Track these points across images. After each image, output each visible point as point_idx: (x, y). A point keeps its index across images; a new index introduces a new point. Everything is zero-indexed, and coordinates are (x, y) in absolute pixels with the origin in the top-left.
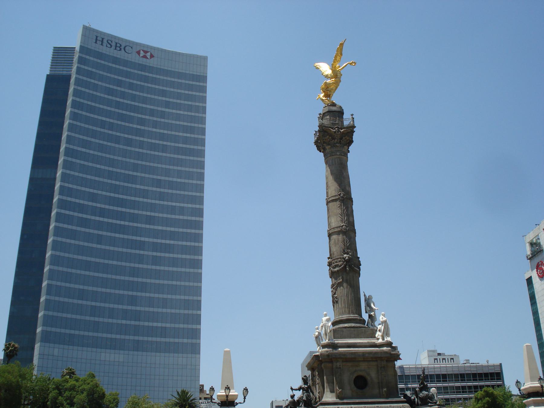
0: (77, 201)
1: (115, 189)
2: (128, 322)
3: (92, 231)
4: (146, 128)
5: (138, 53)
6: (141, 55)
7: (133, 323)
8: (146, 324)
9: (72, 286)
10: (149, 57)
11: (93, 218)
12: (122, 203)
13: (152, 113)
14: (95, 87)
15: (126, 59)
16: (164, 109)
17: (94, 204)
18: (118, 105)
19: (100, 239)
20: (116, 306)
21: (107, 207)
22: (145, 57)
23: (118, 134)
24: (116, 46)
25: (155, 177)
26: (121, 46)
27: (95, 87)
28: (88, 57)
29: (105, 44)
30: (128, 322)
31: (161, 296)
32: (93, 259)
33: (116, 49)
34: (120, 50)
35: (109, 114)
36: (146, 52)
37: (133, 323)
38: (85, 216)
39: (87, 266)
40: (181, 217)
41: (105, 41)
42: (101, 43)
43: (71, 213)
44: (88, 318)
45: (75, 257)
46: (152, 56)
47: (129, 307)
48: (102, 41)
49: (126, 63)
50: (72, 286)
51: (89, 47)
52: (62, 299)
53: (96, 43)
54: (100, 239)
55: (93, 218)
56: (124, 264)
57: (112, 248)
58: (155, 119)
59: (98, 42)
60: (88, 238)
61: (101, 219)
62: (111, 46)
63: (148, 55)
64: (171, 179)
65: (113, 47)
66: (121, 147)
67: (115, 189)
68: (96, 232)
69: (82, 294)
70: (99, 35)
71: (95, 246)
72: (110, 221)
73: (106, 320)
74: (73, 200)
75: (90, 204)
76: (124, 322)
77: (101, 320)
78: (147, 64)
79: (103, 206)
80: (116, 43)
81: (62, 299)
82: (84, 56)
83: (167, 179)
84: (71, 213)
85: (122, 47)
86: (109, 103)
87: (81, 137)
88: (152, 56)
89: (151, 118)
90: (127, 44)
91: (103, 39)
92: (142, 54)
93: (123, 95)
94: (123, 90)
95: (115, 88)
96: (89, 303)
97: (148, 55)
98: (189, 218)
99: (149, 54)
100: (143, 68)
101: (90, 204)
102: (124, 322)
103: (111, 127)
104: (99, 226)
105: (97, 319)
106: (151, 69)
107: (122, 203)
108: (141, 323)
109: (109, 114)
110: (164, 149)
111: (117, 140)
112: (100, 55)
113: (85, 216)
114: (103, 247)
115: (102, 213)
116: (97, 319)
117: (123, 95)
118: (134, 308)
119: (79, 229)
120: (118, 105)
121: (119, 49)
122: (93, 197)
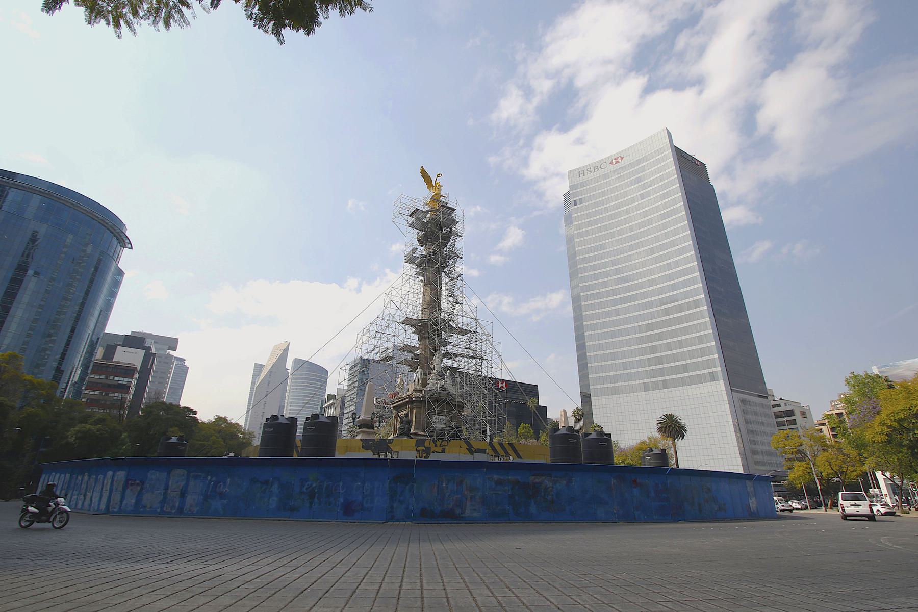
1: (619, 271)
5: (612, 163)
9: (605, 352)
19: (617, 312)
22: (617, 162)
31: (676, 339)
32: (616, 329)
39: (613, 334)
40: (677, 269)
44: (622, 372)
45: (603, 331)
47: (652, 356)
50: (605, 352)
52: (600, 364)
54: (617, 312)
57: (628, 315)
60: (608, 314)
69: (614, 356)
71: (615, 318)
72: (622, 296)
73: (636, 370)
77: (632, 371)
81: (600, 364)
92: (614, 161)
96: (620, 361)
98: (684, 267)
104: (615, 303)
105: (629, 371)
118: (656, 355)
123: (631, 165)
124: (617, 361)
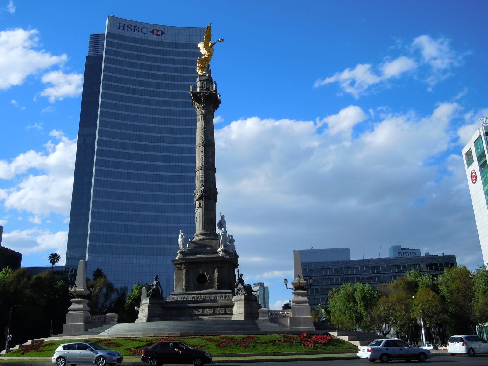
0: (111, 149)
1: (140, 138)
2: (152, 235)
3: (123, 170)
4: (161, 90)
5: (152, 32)
6: (155, 34)
7: (156, 235)
8: (166, 235)
9: (110, 211)
10: (160, 34)
11: (124, 161)
12: (145, 148)
13: (165, 78)
14: (121, 63)
15: (143, 38)
16: (173, 74)
17: (124, 151)
18: (138, 74)
20: (143, 224)
21: (134, 152)
22: (157, 35)
23: (140, 97)
24: (135, 29)
25: (169, 126)
27: (121, 63)
28: (113, 40)
29: (126, 29)
30: (152, 235)
33: (135, 31)
34: (138, 31)
35: (133, 82)
36: (158, 31)
37: (156, 235)
38: (117, 160)
41: (126, 26)
42: (123, 28)
43: (107, 159)
46: (163, 33)
48: (124, 27)
49: (143, 41)
51: (114, 32)
53: (119, 28)
55: (124, 161)
56: (148, 193)
58: (167, 82)
59: (121, 28)
61: (130, 161)
63: (160, 33)
64: (181, 127)
65: (133, 30)
66: (142, 106)
67: (140, 138)
68: (126, 171)
70: (121, 22)
71: (126, 181)
72: (136, 162)
74: (108, 149)
75: (121, 150)
76: (149, 235)
78: (160, 40)
79: (131, 151)
80: (135, 27)
82: (111, 40)
83: (178, 127)
84: (107, 159)
85: (140, 30)
86: (132, 73)
87: (112, 101)
88: (163, 33)
89: (164, 82)
90: (144, 26)
91: (124, 25)
92: (155, 32)
93: (142, 66)
94: (142, 62)
95: (136, 61)
97: (160, 33)
100: (157, 43)
101: (121, 150)
102: (149, 235)
103: (134, 91)
105: (129, 234)
106: (163, 44)
107: (145, 148)
108: (162, 235)
109: (133, 82)
110: (175, 104)
111: (139, 101)
112: (123, 38)
113: (117, 160)
114: (132, 181)
115: (130, 156)
116: (129, 234)
117: (142, 66)
118: (156, 224)
119: (113, 169)
120: (138, 74)
121: (137, 31)
122: (123, 146)
123: (169, 44)
124: (120, 223)
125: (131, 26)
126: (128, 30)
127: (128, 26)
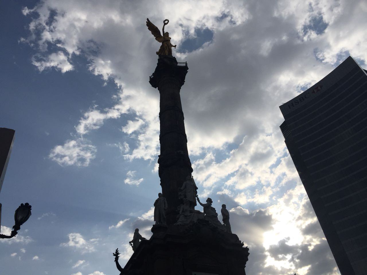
5: (314, 92)
10: (320, 89)
26: (303, 98)
34: (304, 100)
53: (290, 108)
62: (298, 102)
63: (319, 88)
80: (300, 99)
88: (321, 87)
91: (292, 104)
92: (315, 91)
99: (319, 87)
125: (297, 101)
126: (296, 105)
127: (295, 103)
